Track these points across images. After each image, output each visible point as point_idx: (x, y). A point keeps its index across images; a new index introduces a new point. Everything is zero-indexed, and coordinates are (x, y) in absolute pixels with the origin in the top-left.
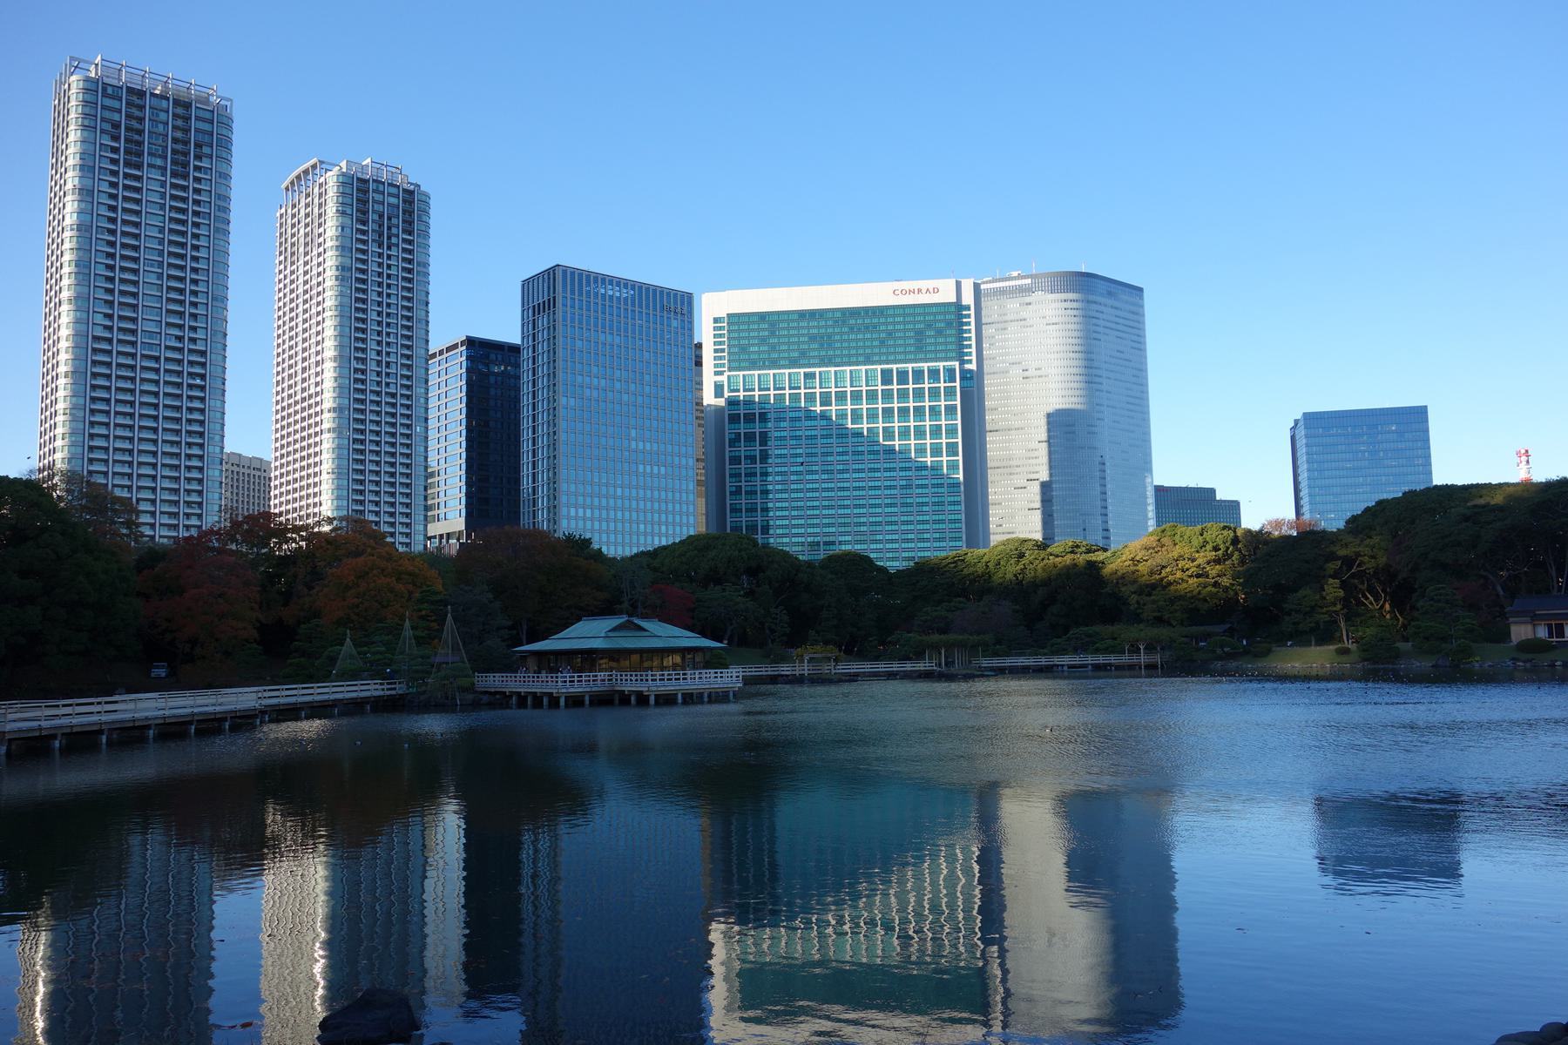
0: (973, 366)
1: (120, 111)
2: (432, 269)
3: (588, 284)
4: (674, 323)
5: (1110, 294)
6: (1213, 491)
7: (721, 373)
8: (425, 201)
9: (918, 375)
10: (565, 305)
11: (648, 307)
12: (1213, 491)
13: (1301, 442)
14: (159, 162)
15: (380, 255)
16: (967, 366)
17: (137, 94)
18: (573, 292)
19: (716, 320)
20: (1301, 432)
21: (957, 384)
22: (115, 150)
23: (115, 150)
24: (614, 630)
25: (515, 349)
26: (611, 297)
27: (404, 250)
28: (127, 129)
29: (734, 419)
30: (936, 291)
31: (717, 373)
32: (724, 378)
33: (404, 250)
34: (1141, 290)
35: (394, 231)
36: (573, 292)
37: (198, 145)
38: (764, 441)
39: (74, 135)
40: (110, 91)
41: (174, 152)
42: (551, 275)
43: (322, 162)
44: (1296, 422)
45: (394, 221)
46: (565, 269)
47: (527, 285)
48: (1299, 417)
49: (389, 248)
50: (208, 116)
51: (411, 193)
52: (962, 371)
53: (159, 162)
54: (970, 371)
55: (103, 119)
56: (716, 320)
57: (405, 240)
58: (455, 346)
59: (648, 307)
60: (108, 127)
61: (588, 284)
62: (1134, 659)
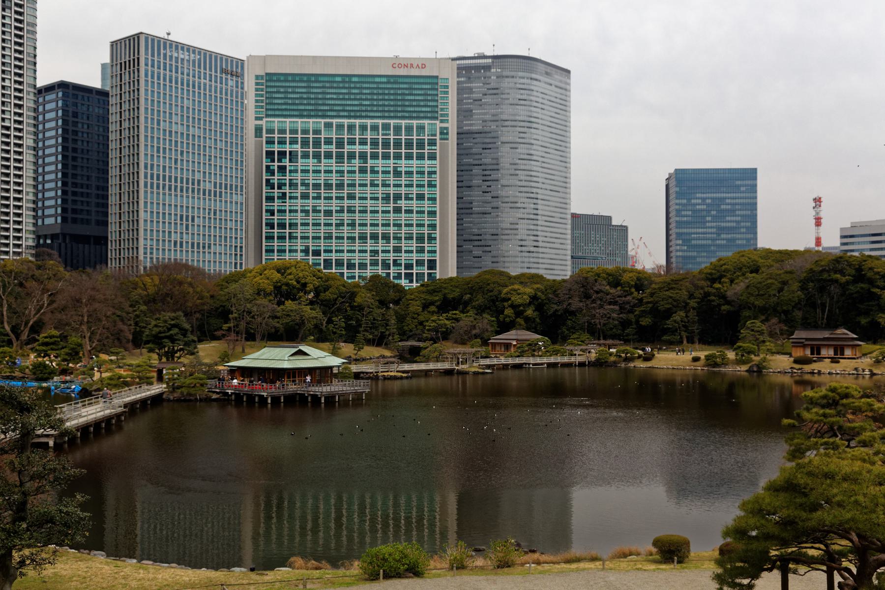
3: (165, 48)
4: (230, 83)
5: (547, 73)
6: (610, 218)
7: (260, 119)
9: (409, 129)
10: (146, 65)
12: (610, 218)
13: (673, 190)
18: (153, 55)
19: (257, 77)
20: (673, 183)
21: (438, 137)
24: (292, 355)
25: (102, 94)
26: (183, 60)
27: (16, 12)
30: (424, 66)
31: (257, 119)
32: (263, 123)
33: (16, 12)
34: (568, 72)
36: (153, 55)
42: (134, 40)
44: (670, 175)
46: (147, 36)
47: (115, 45)
48: (672, 171)
52: (441, 128)
54: (447, 128)
56: (257, 77)
58: (49, 88)
61: (165, 48)
62: (573, 359)
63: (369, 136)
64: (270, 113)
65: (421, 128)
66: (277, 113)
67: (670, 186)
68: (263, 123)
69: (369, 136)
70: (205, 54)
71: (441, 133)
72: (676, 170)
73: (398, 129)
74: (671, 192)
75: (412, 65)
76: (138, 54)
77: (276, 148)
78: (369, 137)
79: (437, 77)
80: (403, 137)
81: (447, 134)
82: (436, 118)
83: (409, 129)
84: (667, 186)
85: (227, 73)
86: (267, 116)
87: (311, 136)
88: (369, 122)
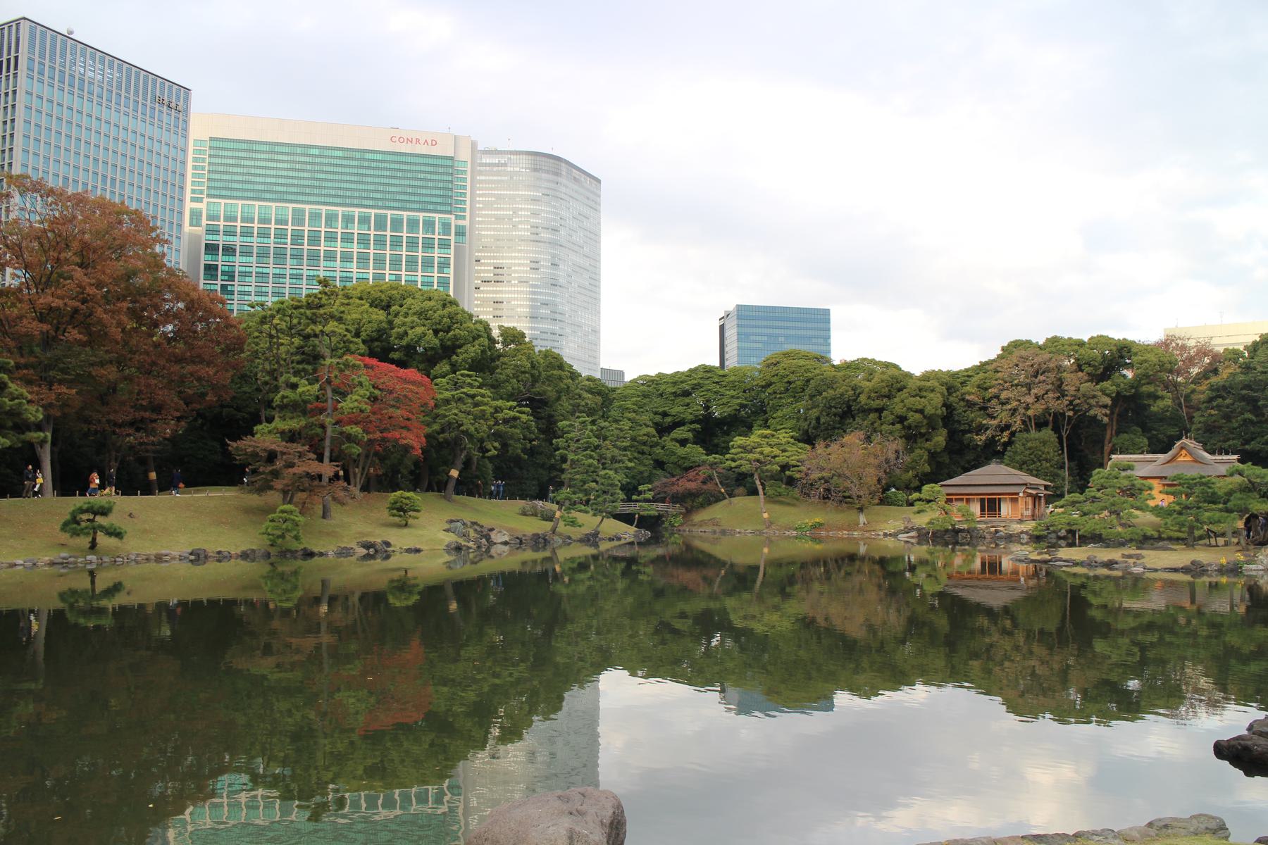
0: (466, 223)
4: (165, 119)
7: (200, 200)
9: (413, 224)
11: (136, 93)
13: (731, 333)
16: (461, 223)
21: (452, 237)
29: (211, 248)
31: (193, 200)
32: (203, 206)
34: (599, 181)
38: (231, 276)
48: (731, 308)
54: (464, 227)
59: (136, 93)
63: (356, 230)
64: (213, 192)
65: (429, 225)
66: (224, 193)
67: (727, 327)
68: (203, 206)
69: (356, 230)
70: (129, 71)
71: (456, 234)
72: (738, 306)
73: (397, 224)
74: (727, 334)
75: (418, 141)
77: (221, 240)
78: (356, 232)
79: (452, 158)
80: (405, 235)
81: (463, 234)
82: (450, 212)
83: (413, 224)
84: (722, 328)
85: (161, 103)
86: (208, 196)
87: (273, 226)
88: (357, 212)
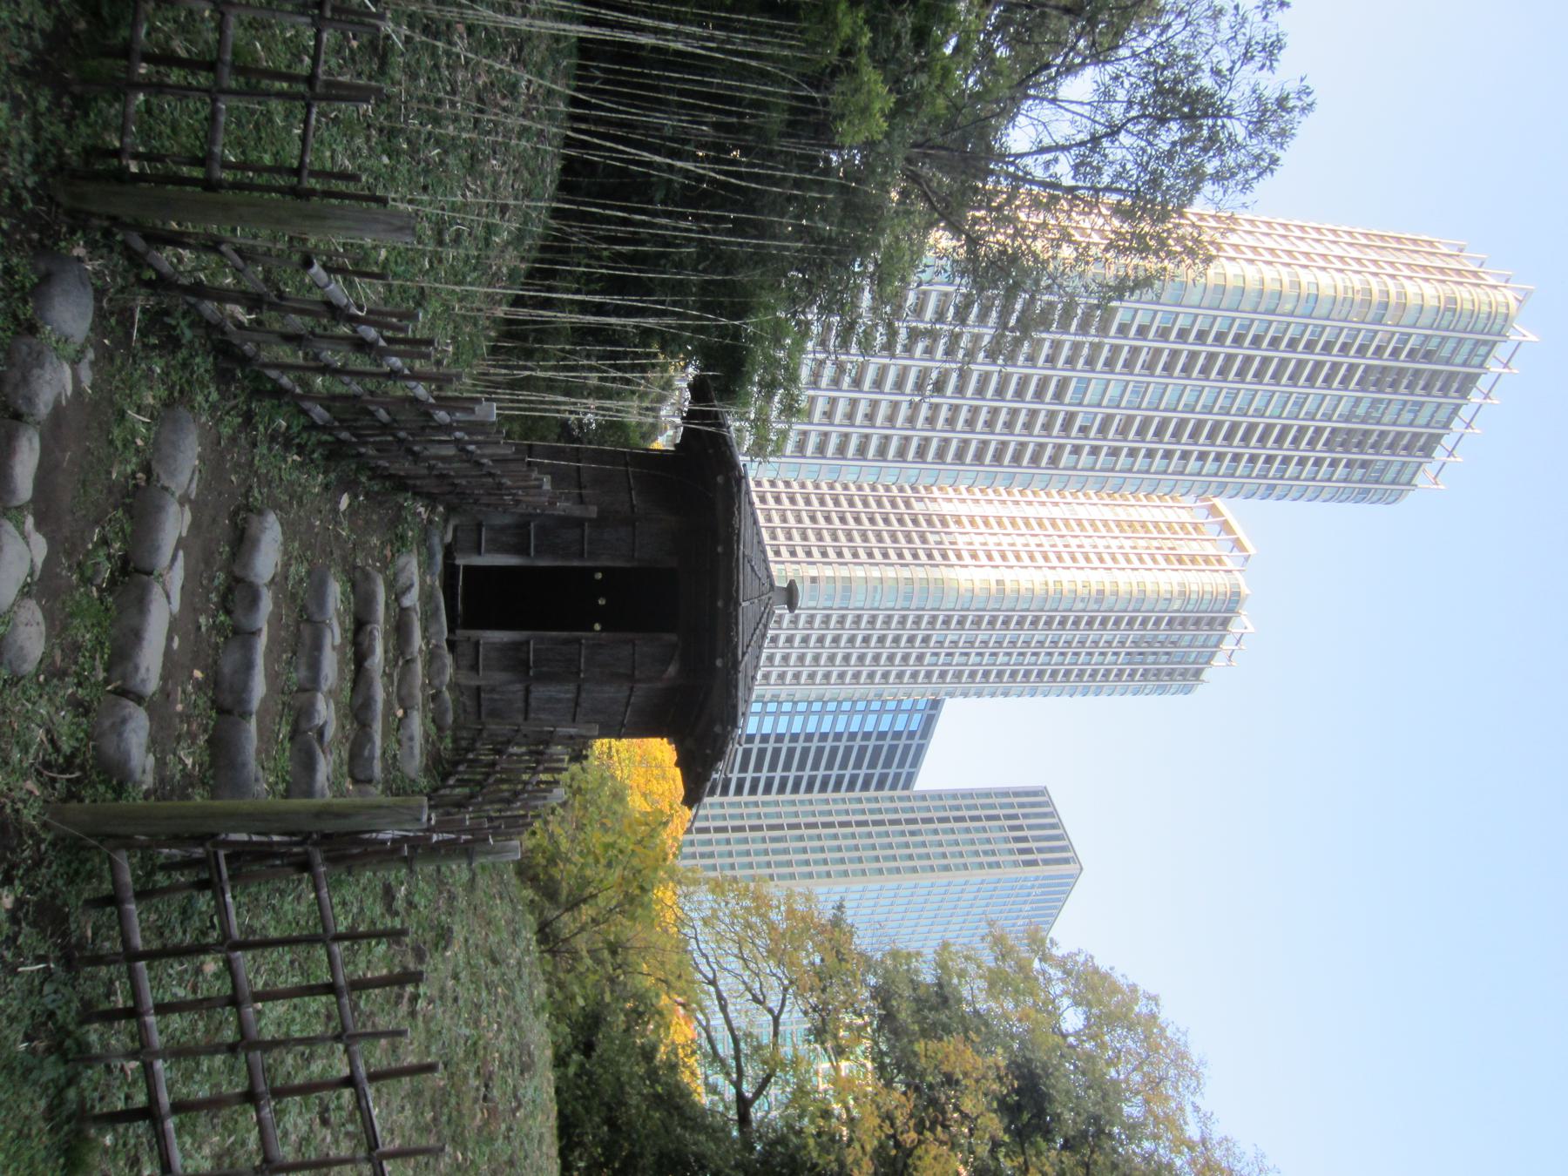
1: (1447, 362)
2: (1090, 698)
8: (1187, 690)
14: (1361, 411)
15: (1122, 644)
17: (1466, 384)
22: (1395, 353)
23: (1395, 353)
28: (1417, 373)
35: (1151, 658)
37: (1364, 464)
39: (1425, 292)
40: (1483, 350)
41: (1366, 433)
43: (1247, 558)
45: (1164, 658)
49: (1128, 654)
50: (1404, 478)
51: (1197, 674)
53: (1361, 411)
55: (1444, 339)
57: (1134, 672)
60: (1432, 345)
76: (1046, 862)
